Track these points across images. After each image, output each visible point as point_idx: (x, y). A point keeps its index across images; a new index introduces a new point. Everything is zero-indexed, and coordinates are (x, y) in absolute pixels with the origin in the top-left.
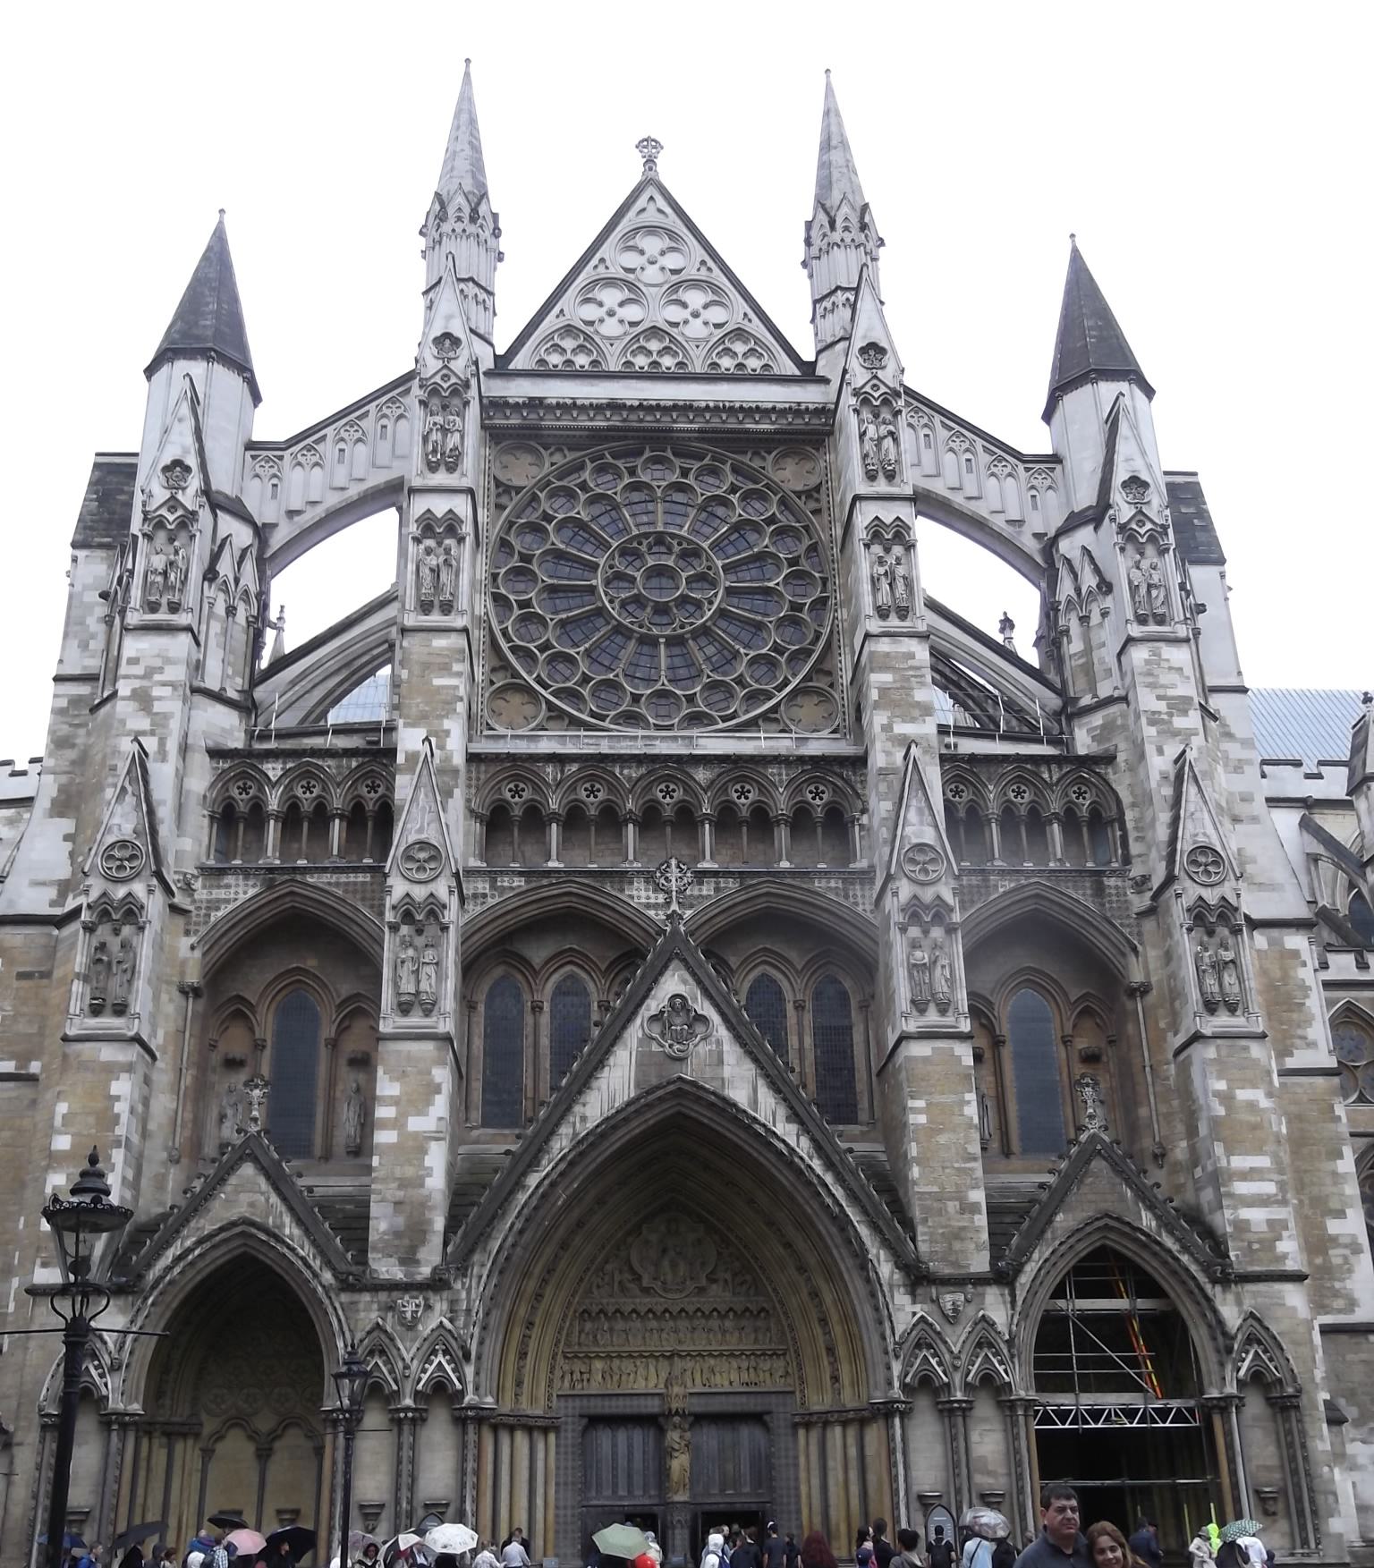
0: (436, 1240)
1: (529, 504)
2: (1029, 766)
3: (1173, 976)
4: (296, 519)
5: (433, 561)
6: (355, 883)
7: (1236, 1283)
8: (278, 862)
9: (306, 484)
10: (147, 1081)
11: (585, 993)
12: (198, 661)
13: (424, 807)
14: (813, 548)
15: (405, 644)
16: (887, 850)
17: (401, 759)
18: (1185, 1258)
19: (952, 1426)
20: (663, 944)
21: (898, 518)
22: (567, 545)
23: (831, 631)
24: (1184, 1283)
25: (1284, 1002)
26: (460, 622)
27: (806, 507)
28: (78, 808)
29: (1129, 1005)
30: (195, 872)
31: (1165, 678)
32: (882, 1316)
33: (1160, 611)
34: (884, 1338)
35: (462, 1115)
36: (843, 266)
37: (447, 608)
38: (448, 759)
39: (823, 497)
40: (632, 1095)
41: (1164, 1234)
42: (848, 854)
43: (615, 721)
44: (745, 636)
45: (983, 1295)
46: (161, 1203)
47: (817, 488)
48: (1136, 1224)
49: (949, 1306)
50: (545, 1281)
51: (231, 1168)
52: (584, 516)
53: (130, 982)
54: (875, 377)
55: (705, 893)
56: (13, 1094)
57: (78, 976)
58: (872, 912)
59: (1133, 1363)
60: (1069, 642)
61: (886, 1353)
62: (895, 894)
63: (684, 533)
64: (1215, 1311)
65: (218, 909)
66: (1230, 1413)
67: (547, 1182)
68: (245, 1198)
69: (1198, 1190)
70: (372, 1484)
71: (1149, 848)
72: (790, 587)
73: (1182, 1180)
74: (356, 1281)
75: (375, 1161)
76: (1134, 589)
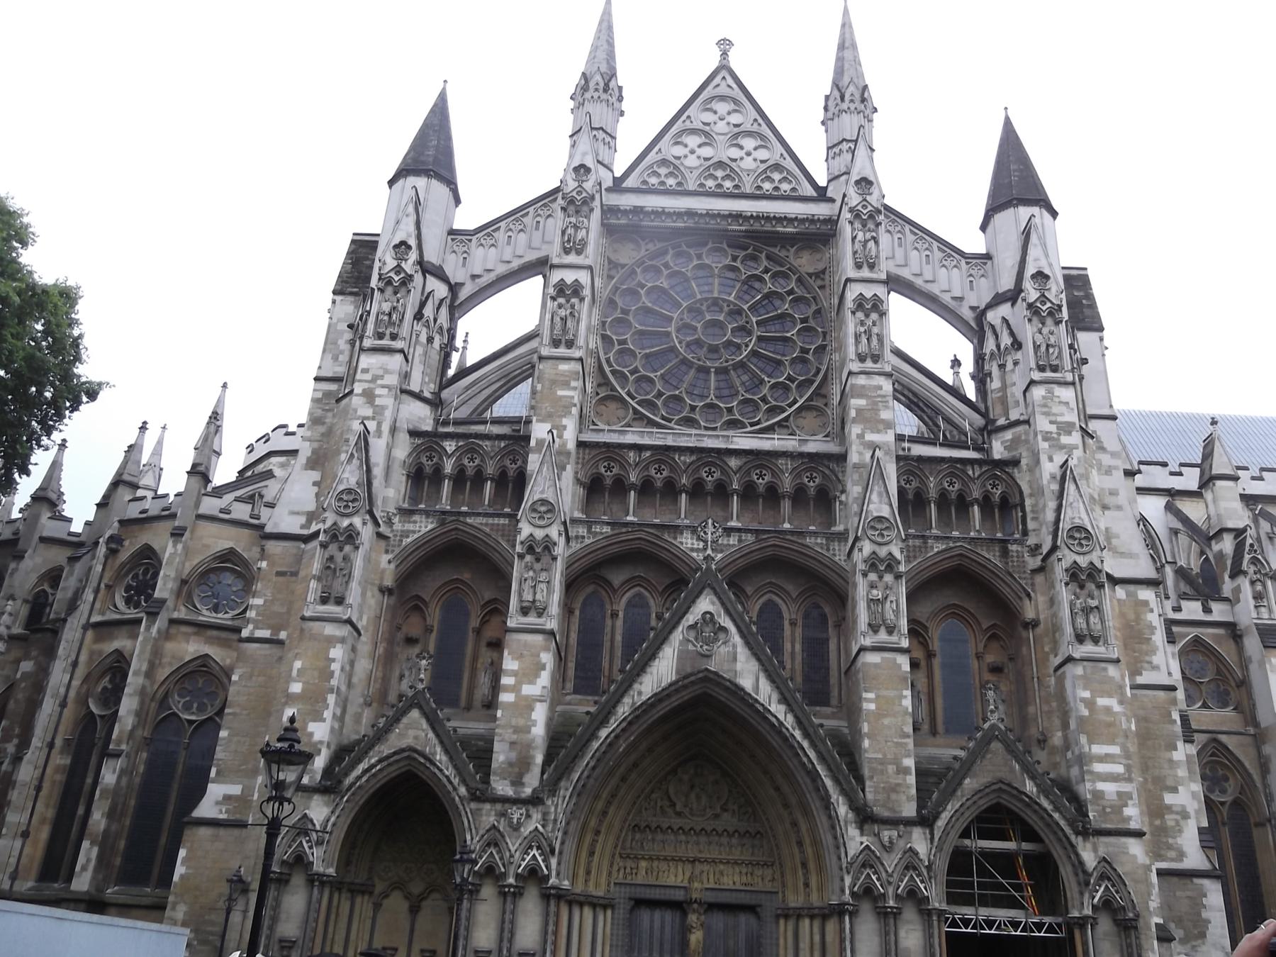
0: (536, 770)
1: (630, 275)
3: (1055, 615)
4: (477, 280)
5: (562, 313)
6: (498, 525)
7: (1093, 836)
8: (448, 507)
9: (485, 259)
10: (354, 649)
11: (647, 606)
12: (406, 372)
13: (546, 477)
14: (818, 312)
15: (541, 367)
16: (856, 520)
17: (533, 443)
18: (1056, 816)
19: (886, 925)
20: (700, 577)
21: (875, 295)
22: (654, 303)
23: (828, 368)
24: (1055, 833)
25: (1136, 637)
26: (577, 354)
27: (815, 284)
28: (323, 465)
29: (1024, 634)
30: (395, 512)
31: (1055, 409)
32: (839, 843)
33: (1055, 363)
34: (840, 859)
35: (560, 685)
36: (848, 125)
37: (570, 344)
38: (564, 444)
39: (827, 277)
40: (674, 679)
41: (1042, 797)
42: (832, 522)
44: (769, 369)
45: (911, 833)
46: (357, 732)
47: (823, 272)
48: (1021, 789)
49: (886, 839)
50: (609, 803)
51: (404, 712)
52: (665, 285)
53: (347, 583)
54: (865, 200)
55: (731, 543)
56: (268, 652)
57: (314, 577)
58: (845, 561)
59: (1019, 888)
60: (991, 381)
61: (841, 869)
62: (861, 550)
63: (731, 298)
64: (1077, 855)
65: (407, 537)
66: (1086, 930)
67: (613, 735)
68: (411, 733)
69: (1069, 767)
71: (1041, 525)
72: (801, 337)
73: (1058, 760)
74: (481, 794)
75: (499, 713)
76: (1037, 348)
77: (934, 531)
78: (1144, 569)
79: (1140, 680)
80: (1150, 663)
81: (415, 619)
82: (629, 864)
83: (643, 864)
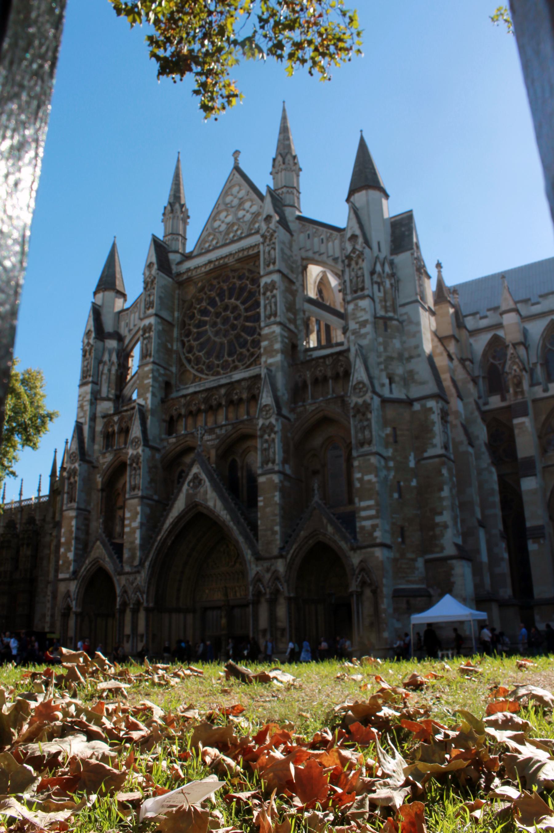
2: (321, 360)
5: (145, 342)
37: (150, 356)
43: (213, 375)
70: (128, 630)
75: (125, 537)
76: (351, 281)
78: (431, 388)
79: (426, 455)
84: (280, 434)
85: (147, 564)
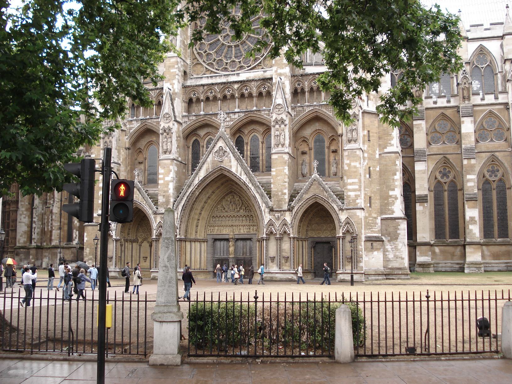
2: (317, 76)
17: (164, 91)
32: (263, 219)
35: (187, 173)
38: (174, 90)
75: (159, 187)
77: (307, 104)
79: (386, 150)
80: (390, 143)
81: (140, 155)
82: (212, 228)
83: (216, 228)
84: (288, 126)
85: (180, 208)
